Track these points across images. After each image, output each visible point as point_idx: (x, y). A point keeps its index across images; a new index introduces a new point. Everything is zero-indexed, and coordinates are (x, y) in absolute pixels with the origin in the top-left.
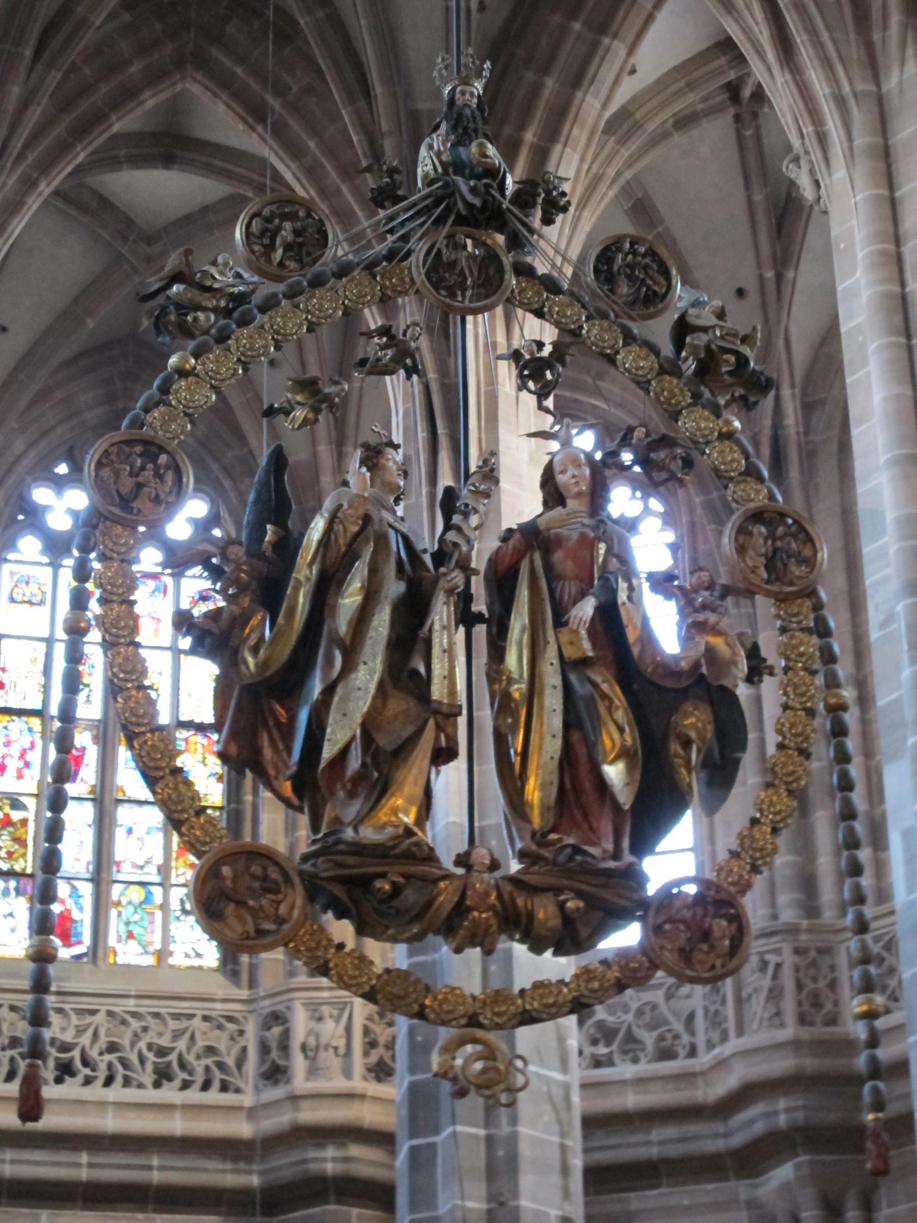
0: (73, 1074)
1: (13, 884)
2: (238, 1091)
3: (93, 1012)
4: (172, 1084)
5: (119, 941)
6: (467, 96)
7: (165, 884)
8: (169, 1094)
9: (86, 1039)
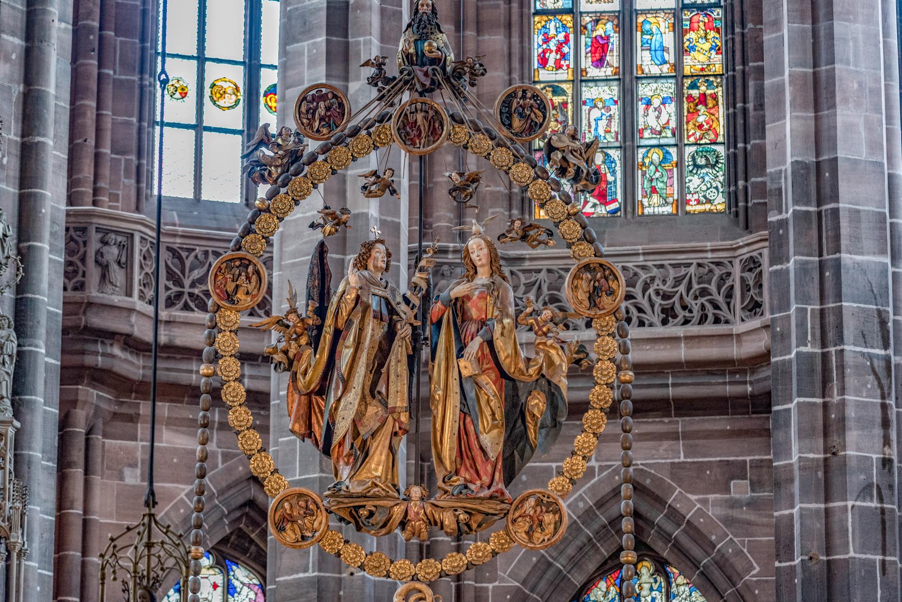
2: (727, 322)
4: (676, 321)
5: (644, 197)
6: (425, 7)
8: (674, 330)
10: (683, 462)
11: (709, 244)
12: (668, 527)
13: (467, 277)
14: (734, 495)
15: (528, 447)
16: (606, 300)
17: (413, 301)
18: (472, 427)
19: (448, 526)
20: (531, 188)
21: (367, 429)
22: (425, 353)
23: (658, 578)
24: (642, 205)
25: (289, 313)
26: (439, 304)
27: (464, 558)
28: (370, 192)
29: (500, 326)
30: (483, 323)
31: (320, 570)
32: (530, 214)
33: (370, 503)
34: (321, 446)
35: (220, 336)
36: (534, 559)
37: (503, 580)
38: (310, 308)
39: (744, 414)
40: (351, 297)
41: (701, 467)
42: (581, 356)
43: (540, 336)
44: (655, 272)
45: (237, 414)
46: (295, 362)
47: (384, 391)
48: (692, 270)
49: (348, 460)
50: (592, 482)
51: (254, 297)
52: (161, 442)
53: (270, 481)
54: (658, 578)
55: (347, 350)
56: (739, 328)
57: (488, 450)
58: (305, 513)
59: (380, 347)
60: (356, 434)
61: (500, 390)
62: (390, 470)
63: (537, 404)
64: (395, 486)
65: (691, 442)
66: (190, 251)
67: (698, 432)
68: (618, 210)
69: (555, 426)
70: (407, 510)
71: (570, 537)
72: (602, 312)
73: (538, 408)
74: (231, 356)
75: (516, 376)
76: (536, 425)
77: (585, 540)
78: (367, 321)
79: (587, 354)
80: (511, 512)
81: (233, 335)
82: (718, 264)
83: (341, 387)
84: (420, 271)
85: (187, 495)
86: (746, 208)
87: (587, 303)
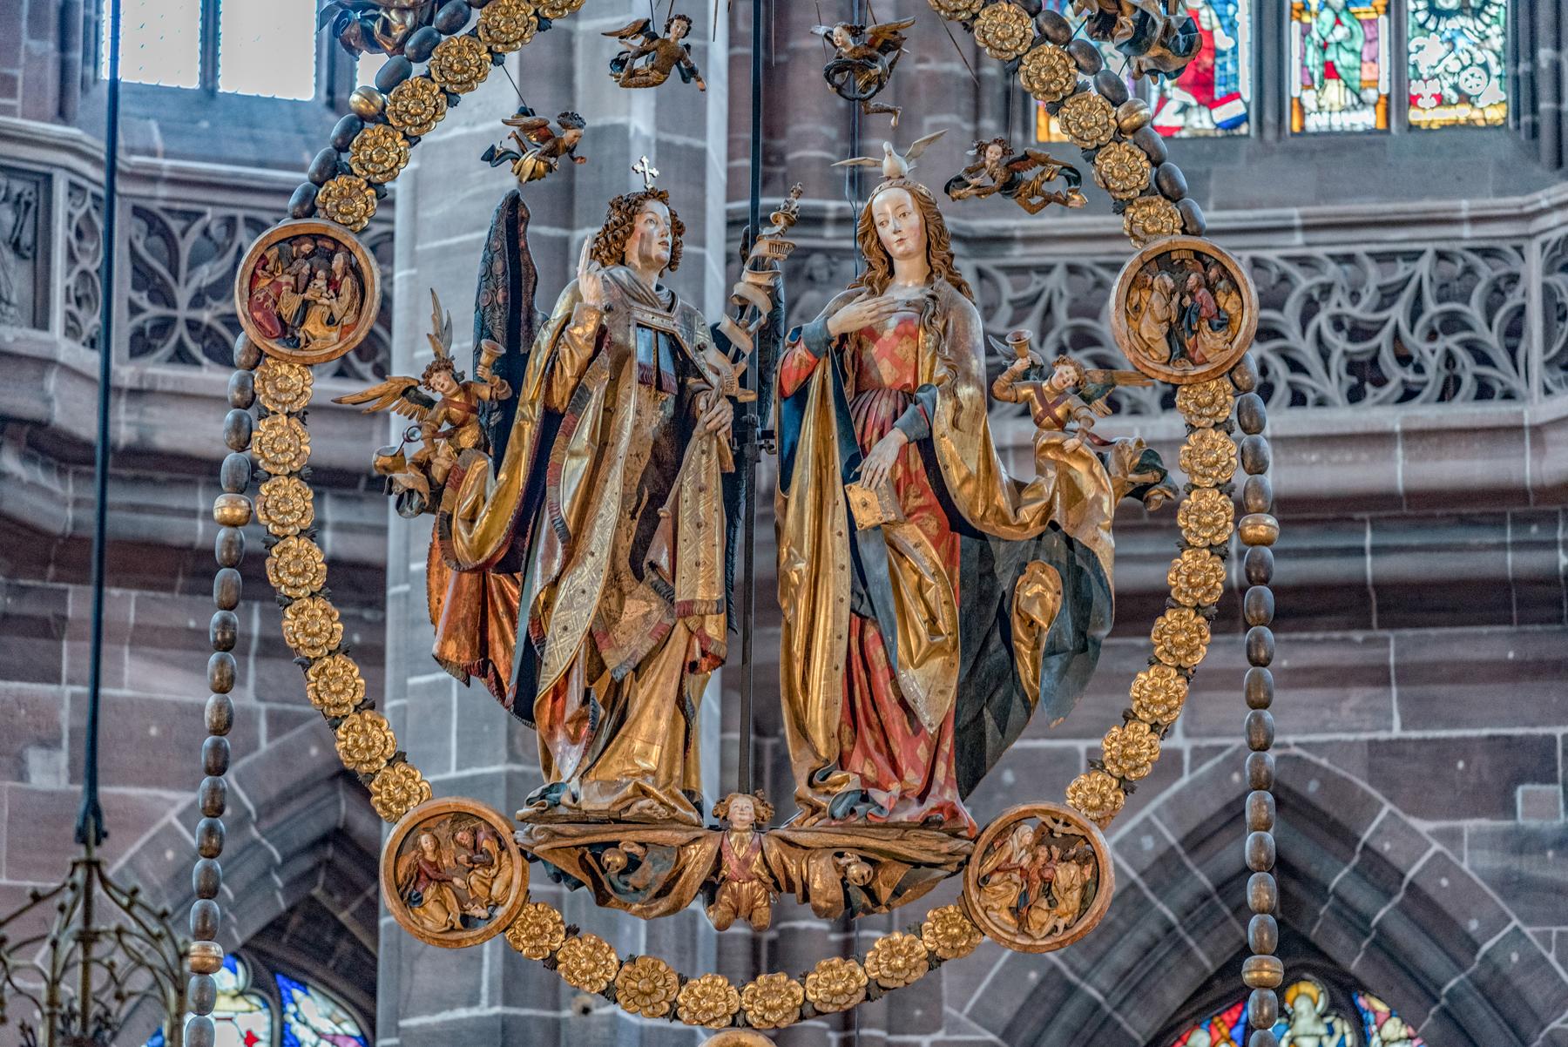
2: (1509, 396)
8: (1378, 414)
10: (1399, 741)
11: (1464, 204)
12: (1362, 897)
13: (870, 283)
14: (1525, 819)
15: (1017, 700)
16: (1210, 342)
17: (736, 343)
18: (881, 651)
19: (821, 894)
20: (1028, 66)
21: (623, 655)
22: (766, 469)
23: (1338, 1025)
24: (1301, 107)
25: (431, 370)
26: (800, 350)
27: (859, 972)
28: (633, 74)
29: (950, 403)
30: (908, 396)
31: (507, 1002)
32: (1026, 128)
34: (510, 696)
35: (263, 425)
36: (1033, 976)
37: (955, 1027)
38: (484, 358)
39: (1550, 621)
40: (584, 330)
41: (1444, 751)
42: (1149, 477)
43: (1048, 428)
44: (1332, 272)
45: (305, 618)
46: (448, 491)
47: (664, 561)
48: (1424, 267)
49: (577, 731)
50: (1176, 786)
51: (346, 330)
52: (120, 686)
53: (385, 782)
54: (1338, 1025)
55: (574, 462)
56: (1536, 409)
57: (921, 708)
58: (470, 860)
59: (654, 455)
60: (597, 667)
61: (949, 560)
62: (680, 755)
63: (1039, 595)
64: (690, 794)
65: (1417, 690)
66: (191, 216)
67: (1435, 666)
68: (1244, 118)
69: (1085, 649)
70: (720, 853)
71: (1121, 924)
72: (1200, 370)
73: (1043, 605)
74: (290, 475)
75: (989, 526)
76: (1037, 646)
77: (1157, 930)
78: (623, 390)
79: (1164, 474)
80: (975, 859)
81: (294, 422)
82: (1487, 253)
83: (560, 552)
84: (754, 268)
85: (182, 817)
86: (1558, 115)
87: (1162, 348)
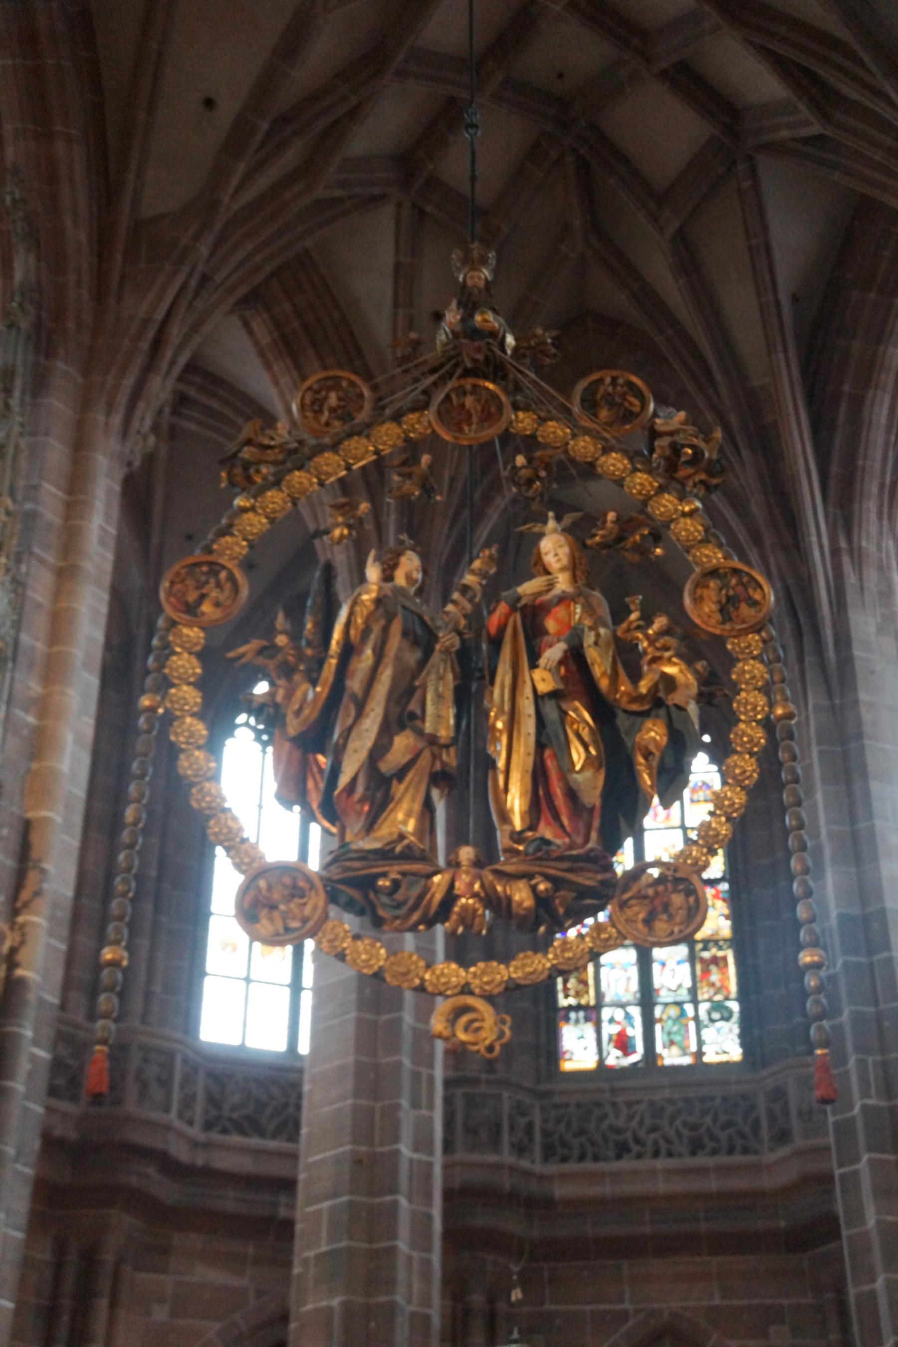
0: (629, 1151)
1: (581, 1014)
2: (756, 1152)
3: (638, 1102)
7: (695, 1002)
8: (702, 1160)
9: (634, 1123)
33: (397, 868)
56: (769, 1157)
82: (744, 1097)
